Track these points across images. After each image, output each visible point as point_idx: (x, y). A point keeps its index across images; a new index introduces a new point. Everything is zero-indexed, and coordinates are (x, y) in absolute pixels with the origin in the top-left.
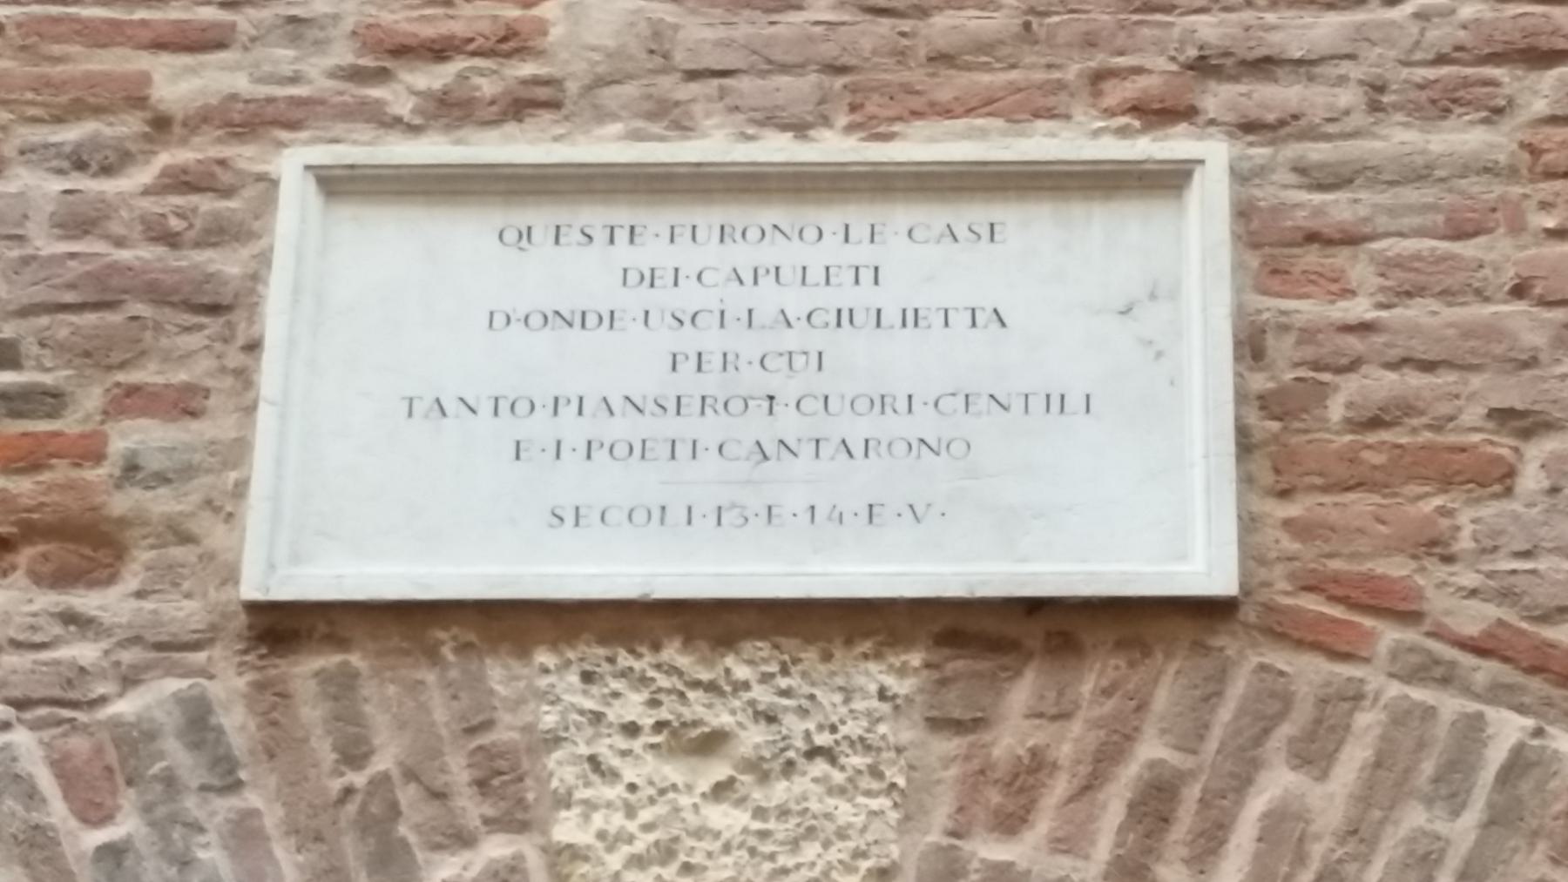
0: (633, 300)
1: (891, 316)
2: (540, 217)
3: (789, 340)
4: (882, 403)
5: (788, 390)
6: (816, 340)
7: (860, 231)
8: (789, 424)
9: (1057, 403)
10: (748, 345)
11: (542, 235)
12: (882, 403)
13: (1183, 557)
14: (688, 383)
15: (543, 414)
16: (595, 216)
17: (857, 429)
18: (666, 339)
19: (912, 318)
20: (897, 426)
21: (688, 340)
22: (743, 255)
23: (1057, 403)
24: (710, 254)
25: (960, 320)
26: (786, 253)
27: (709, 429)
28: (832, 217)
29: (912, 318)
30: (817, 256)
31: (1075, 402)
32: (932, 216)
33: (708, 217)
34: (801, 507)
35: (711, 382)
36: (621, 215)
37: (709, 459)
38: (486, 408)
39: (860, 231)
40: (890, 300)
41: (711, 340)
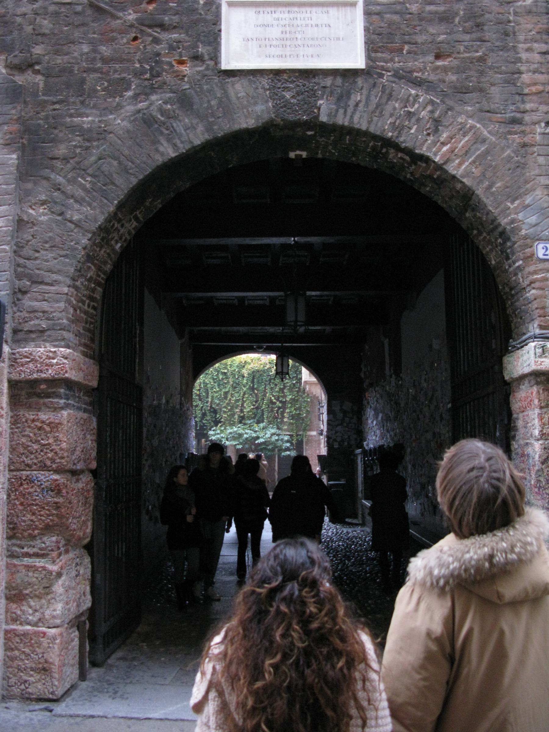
0: (275, 23)
1: (314, 25)
2: (261, 9)
3: (299, 29)
4: (313, 39)
5: (299, 36)
6: (304, 29)
7: (308, 12)
8: (300, 42)
9: (338, 39)
10: (293, 30)
11: (261, 12)
12: (313, 39)
13: (357, 62)
14: (284, 36)
15: (263, 40)
16: (269, 9)
17: (311, 42)
18: (281, 29)
19: (317, 25)
20: (316, 43)
21: (284, 29)
22: (292, 16)
23: (338, 39)
24: (286, 15)
25: (324, 26)
26: (299, 16)
27: (288, 43)
28: (303, 9)
29: (317, 25)
30: (302, 16)
31: (341, 39)
32: (320, 9)
33: (287, 9)
34: (302, 54)
35: (288, 36)
36: (273, 9)
37: (288, 48)
38: (255, 40)
39: (308, 12)
40: (313, 22)
41: (288, 29)
